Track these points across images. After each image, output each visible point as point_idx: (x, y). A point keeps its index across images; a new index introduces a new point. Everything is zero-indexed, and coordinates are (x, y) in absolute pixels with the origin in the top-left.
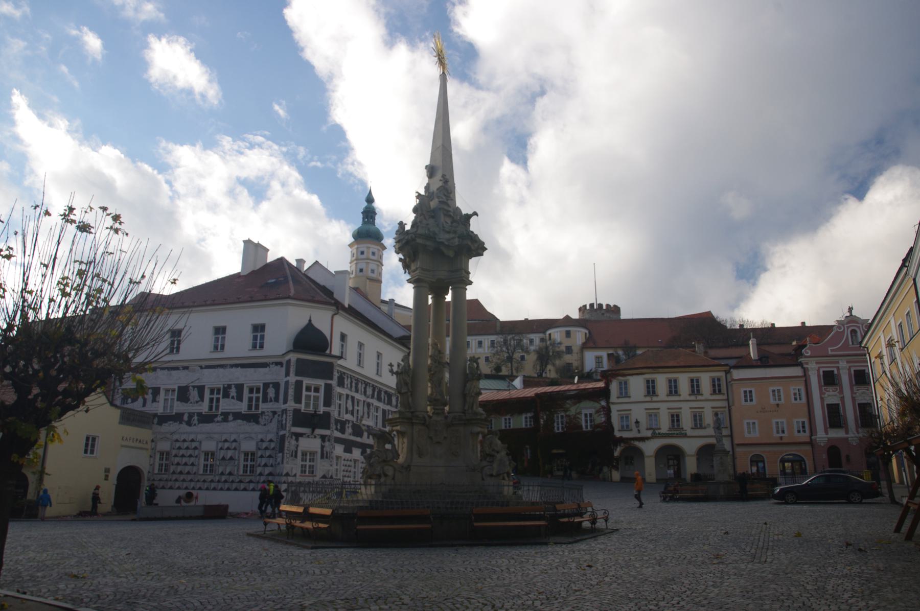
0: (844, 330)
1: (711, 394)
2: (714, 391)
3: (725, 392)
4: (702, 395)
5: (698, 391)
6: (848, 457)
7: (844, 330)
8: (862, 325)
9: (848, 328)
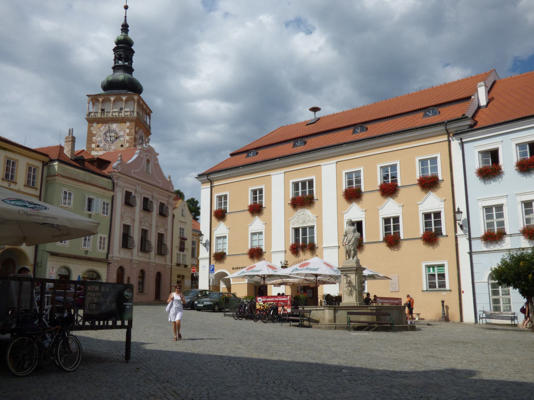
0: (144, 156)
1: (25, 185)
2: (28, 181)
3: (39, 187)
4: (16, 183)
5: (12, 177)
6: (129, 278)
7: (144, 156)
8: (154, 157)
9: (147, 155)
